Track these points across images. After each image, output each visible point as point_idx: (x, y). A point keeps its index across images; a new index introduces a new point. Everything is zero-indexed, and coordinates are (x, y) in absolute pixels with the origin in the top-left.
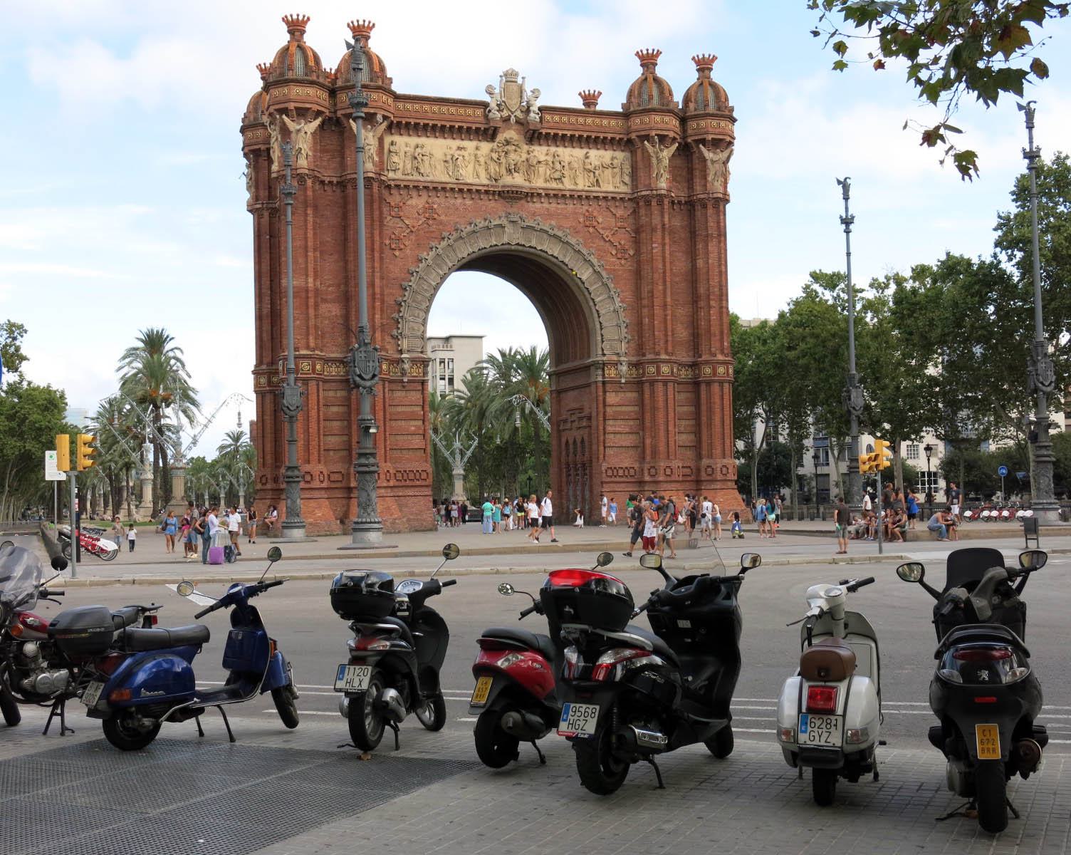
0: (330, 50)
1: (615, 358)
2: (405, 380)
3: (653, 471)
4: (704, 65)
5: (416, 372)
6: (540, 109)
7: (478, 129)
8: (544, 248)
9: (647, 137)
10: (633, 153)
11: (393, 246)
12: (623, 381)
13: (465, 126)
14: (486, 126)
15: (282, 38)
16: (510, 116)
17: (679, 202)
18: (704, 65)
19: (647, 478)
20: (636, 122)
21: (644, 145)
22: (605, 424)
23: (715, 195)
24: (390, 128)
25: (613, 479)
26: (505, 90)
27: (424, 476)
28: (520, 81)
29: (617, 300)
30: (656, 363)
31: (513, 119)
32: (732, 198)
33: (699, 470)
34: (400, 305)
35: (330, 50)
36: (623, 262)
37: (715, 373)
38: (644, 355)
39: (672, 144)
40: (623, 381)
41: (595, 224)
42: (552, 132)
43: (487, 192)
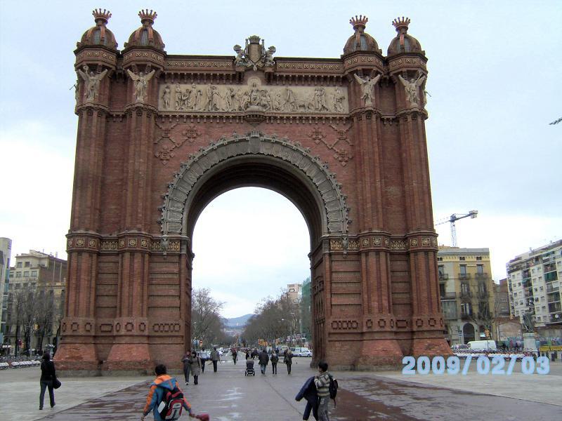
0: (122, 31)
2: (165, 253)
3: (369, 323)
4: (402, 27)
5: (176, 247)
6: (276, 59)
7: (228, 76)
9: (356, 72)
10: (349, 87)
11: (162, 157)
12: (345, 252)
16: (253, 66)
17: (388, 119)
18: (402, 27)
19: (365, 329)
21: (354, 78)
22: (331, 286)
23: (412, 110)
24: (163, 77)
25: (338, 331)
26: (249, 48)
27: (177, 328)
28: (261, 43)
29: (338, 191)
30: (371, 235)
31: (255, 68)
33: (411, 322)
34: (164, 199)
35: (122, 31)
36: (344, 163)
37: (419, 244)
38: (360, 231)
39: (376, 75)
40: (345, 252)
41: (320, 137)
42: (285, 75)
43: (234, 118)
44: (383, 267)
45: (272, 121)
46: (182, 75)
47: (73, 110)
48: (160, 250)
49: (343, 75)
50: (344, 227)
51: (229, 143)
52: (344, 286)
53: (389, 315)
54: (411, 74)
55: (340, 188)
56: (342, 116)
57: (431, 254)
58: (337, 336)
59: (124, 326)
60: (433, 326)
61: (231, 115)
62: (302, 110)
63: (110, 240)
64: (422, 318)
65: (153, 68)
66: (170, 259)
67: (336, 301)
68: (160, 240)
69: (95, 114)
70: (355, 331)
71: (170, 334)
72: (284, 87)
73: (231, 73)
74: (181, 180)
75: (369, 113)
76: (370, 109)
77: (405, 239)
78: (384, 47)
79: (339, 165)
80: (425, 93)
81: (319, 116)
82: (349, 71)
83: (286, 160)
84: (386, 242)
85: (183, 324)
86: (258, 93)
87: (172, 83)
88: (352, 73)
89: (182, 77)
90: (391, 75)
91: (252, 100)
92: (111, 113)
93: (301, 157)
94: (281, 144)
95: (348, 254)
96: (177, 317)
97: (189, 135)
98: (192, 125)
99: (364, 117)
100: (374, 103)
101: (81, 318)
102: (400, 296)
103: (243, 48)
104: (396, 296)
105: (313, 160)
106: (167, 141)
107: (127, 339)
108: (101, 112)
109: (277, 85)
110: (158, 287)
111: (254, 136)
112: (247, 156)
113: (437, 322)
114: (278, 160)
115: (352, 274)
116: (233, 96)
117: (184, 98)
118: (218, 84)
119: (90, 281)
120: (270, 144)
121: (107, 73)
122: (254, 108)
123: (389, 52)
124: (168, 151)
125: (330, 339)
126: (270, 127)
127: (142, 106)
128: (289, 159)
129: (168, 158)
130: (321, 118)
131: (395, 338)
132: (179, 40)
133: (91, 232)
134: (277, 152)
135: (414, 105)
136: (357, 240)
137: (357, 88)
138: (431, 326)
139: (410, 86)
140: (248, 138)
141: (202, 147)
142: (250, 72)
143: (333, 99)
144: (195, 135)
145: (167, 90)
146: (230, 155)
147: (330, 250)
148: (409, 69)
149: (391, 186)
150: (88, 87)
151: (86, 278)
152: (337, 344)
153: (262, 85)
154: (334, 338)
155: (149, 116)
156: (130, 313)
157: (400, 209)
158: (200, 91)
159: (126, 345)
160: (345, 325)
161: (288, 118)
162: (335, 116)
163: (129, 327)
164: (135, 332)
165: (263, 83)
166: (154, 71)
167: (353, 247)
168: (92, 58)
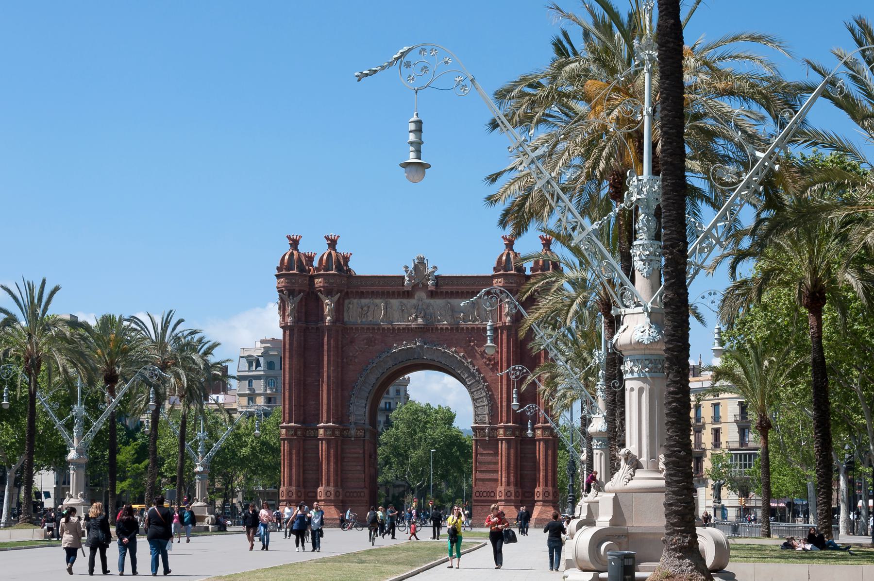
6: (437, 277)
15: (287, 249)
19: (498, 498)
25: (479, 498)
26: (416, 266)
27: (362, 494)
31: (421, 285)
46: (362, 292)
47: (278, 325)
61: (401, 327)
63: (312, 429)
67: (479, 476)
69: (296, 331)
84: (517, 433)
85: (366, 491)
89: (362, 295)
146: (400, 359)
150: (289, 309)
156: (328, 485)
163: (329, 494)
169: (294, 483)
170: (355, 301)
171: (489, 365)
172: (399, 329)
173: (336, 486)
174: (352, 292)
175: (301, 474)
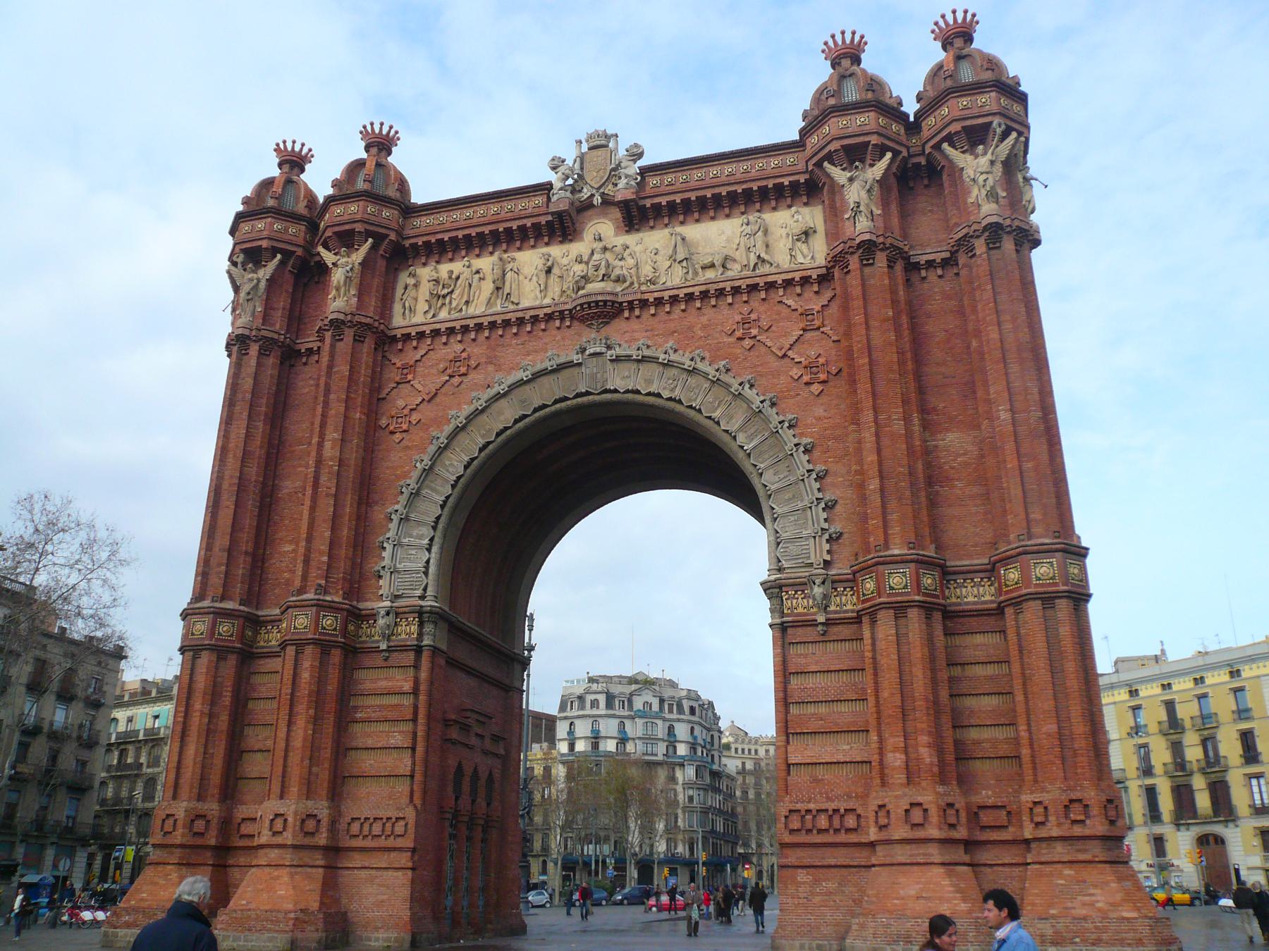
1: (804, 573)
2: (383, 646)
4: (957, 36)
5: (408, 631)
6: (644, 171)
7: (536, 226)
8: (653, 389)
13: (514, 225)
14: (550, 218)
16: (593, 195)
17: (930, 264)
18: (957, 36)
19: (873, 834)
20: (814, 140)
22: (787, 712)
23: (984, 223)
26: (582, 158)
27: (399, 828)
31: (597, 200)
32: (1044, 235)
36: (816, 388)
39: (882, 156)
40: (821, 619)
41: (754, 332)
42: (664, 201)
43: (549, 317)
44: (917, 651)
45: (637, 312)
48: (377, 638)
49: (807, 176)
50: (818, 552)
51: (537, 376)
52: (823, 709)
53: (940, 789)
54: (975, 136)
55: (806, 451)
56: (809, 273)
57: (1063, 605)
58: (800, 853)
59: (268, 822)
60: (1082, 822)
61: (541, 313)
62: (710, 274)
64: (1045, 797)
65: (369, 234)
66: (397, 658)
68: (373, 616)
69: (254, 349)
70: (853, 838)
71: (382, 842)
72: (666, 231)
73: (543, 220)
74: (428, 471)
75: (868, 249)
76: (867, 237)
77: (991, 571)
78: (907, 89)
79: (805, 393)
80: (1027, 180)
81: (749, 282)
82: (815, 160)
83: (670, 399)
84: (927, 581)
86: (608, 255)
87: (424, 264)
88: (819, 165)
90: (928, 150)
91: (591, 272)
92: (297, 347)
93: (707, 385)
94: (654, 360)
95: (828, 623)
96: (405, 800)
97: (449, 371)
98: (459, 347)
99: (854, 262)
100: (880, 223)
101: (185, 804)
102: (986, 734)
103: (569, 162)
104: (974, 734)
105: (735, 386)
106: (405, 389)
107: (274, 854)
108: (267, 345)
109: (652, 228)
110: (374, 728)
111: (592, 351)
112: (579, 400)
113: (1095, 811)
114: (651, 400)
115: (845, 677)
116: (549, 271)
117: (446, 291)
118: (519, 249)
119: (211, 716)
120: (634, 366)
121: (282, 262)
122: (592, 287)
123: (919, 98)
124: (406, 411)
125: (784, 861)
126: (634, 324)
127: (341, 317)
128: (676, 394)
129: (405, 427)
130: (753, 288)
131: (967, 859)
132: (434, 172)
133: (229, 605)
134: (649, 382)
135: (989, 211)
136: (852, 581)
137: (837, 198)
138: (1075, 822)
139: (976, 167)
140: (576, 358)
141: (474, 394)
142: (590, 212)
143: (789, 238)
144: (463, 370)
145: (411, 281)
147: (782, 614)
148: (968, 123)
149: (947, 430)
151: (206, 711)
152: (802, 876)
153: (616, 235)
154: (793, 857)
155: (358, 339)
157: (975, 490)
158: (478, 272)
159: (268, 870)
160: (823, 822)
161: (674, 300)
162: (789, 276)
163: (279, 825)
164: (288, 838)
165: (618, 231)
166: (370, 240)
167: (847, 603)
168: (254, 235)
169: (185, 791)
170: (425, 273)
171: (807, 384)
172: (535, 319)
173: (309, 793)
174: (414, 246)
175: (218, 762)
